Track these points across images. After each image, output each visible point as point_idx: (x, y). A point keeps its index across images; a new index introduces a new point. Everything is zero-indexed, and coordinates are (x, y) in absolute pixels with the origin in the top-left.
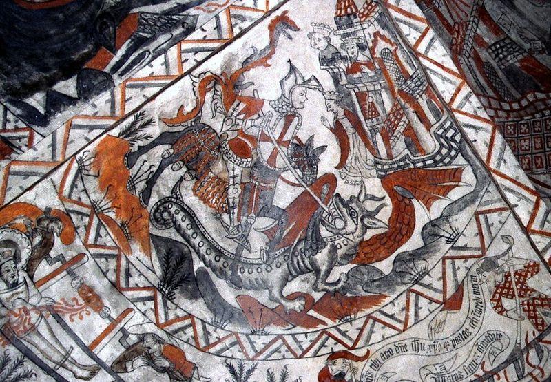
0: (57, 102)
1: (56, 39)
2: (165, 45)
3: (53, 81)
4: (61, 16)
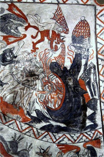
0: (92, 118)
1: (73, 105)
2: (94, 78)
3: (85, 115)
4: (67, 100)
